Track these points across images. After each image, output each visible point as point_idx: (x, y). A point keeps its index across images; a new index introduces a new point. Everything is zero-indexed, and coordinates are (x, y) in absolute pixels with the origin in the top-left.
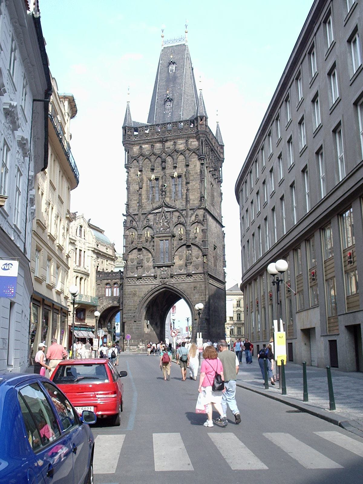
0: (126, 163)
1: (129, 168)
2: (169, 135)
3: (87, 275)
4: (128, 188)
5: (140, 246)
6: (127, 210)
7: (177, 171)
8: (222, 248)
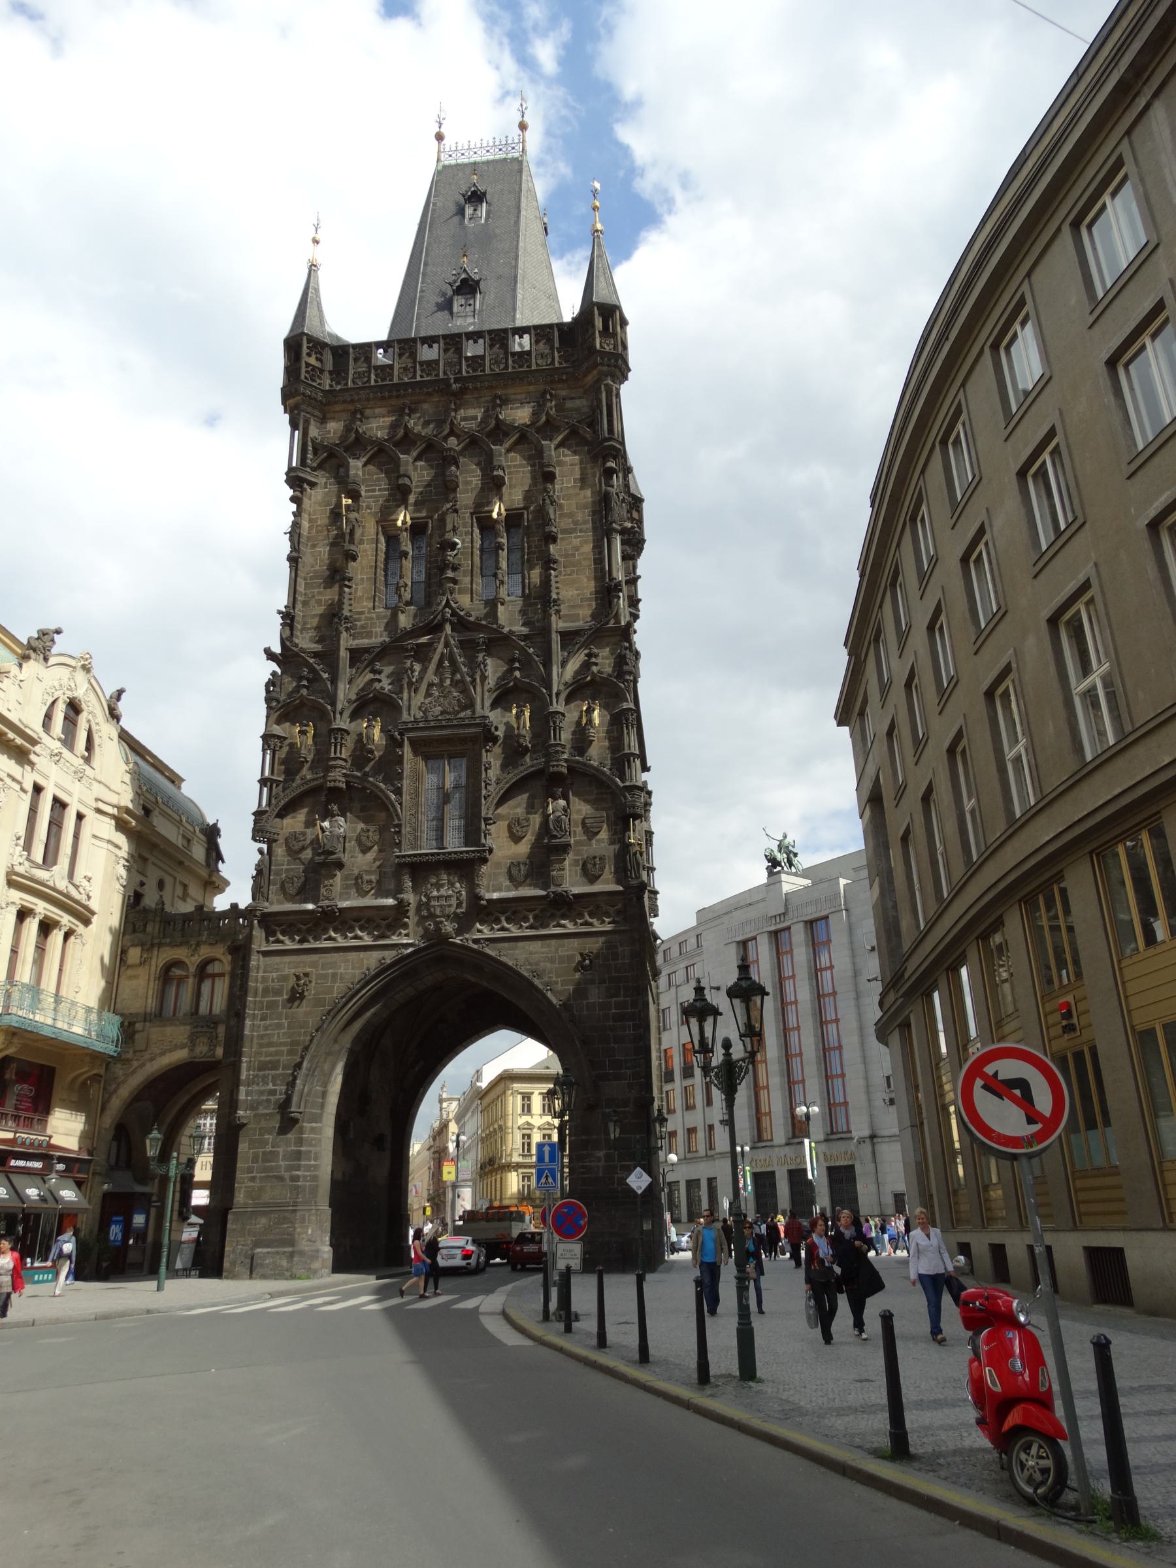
0: (294, 464)
1: (305, 486)
3: (84, 916)
4: (294, 554)
5: (337, 778)
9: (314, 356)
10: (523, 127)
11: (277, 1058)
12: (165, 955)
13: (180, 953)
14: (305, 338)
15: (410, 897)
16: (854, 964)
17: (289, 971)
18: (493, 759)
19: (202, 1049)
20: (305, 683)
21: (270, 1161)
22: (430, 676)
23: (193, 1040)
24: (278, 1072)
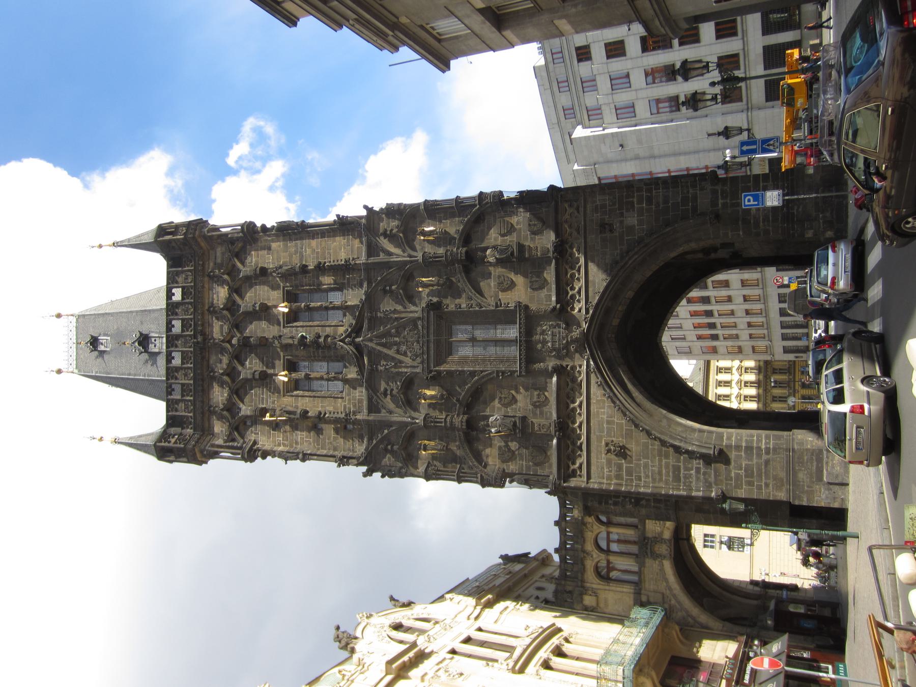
1: (255, 447)
4: (301, 456)
6: (355, 461)
7: (275, 303)
9: (171, 439)
10: (59, 316)
11: (671, 467)
12: (591, 578)
13: (589, 565)
14: (158, 444)
16: (631, 159)
17: (603, 458)
19: (663, 549)
20: (389, 447)
21: (753, 471)
22: (391, 352)
23: (656, 556)
24: (682, 466)
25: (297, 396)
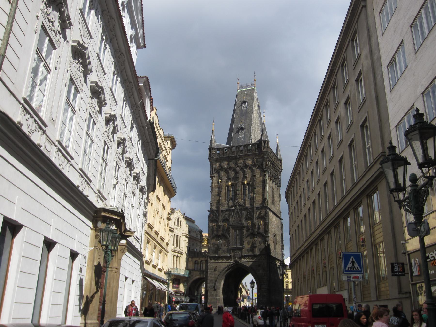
1: (213, 177)
2: (242, 154)
3: (182, 254)
8: (281, 235)
13: (197, 259)
15: (232, 254)
17: (214, 266)
18: (245, 231)
19: (202, 276)
23: (200, 274)
25: (226, 188)
